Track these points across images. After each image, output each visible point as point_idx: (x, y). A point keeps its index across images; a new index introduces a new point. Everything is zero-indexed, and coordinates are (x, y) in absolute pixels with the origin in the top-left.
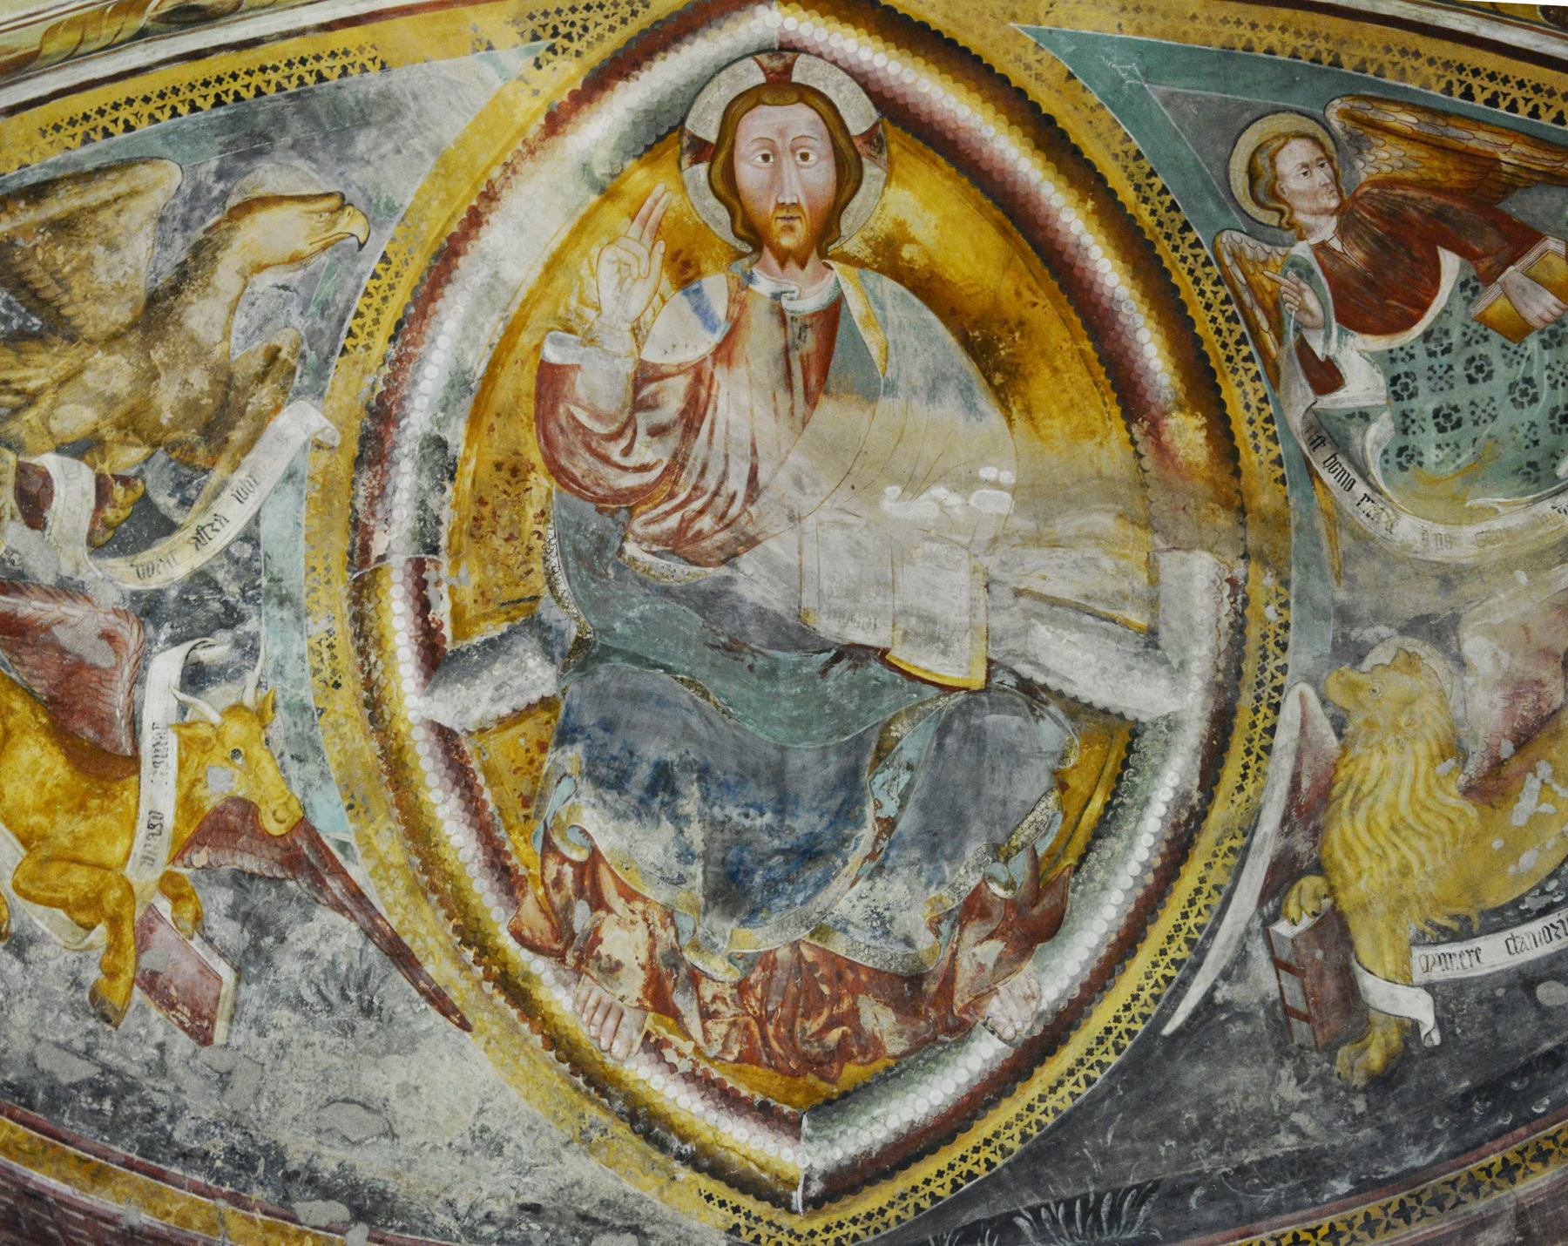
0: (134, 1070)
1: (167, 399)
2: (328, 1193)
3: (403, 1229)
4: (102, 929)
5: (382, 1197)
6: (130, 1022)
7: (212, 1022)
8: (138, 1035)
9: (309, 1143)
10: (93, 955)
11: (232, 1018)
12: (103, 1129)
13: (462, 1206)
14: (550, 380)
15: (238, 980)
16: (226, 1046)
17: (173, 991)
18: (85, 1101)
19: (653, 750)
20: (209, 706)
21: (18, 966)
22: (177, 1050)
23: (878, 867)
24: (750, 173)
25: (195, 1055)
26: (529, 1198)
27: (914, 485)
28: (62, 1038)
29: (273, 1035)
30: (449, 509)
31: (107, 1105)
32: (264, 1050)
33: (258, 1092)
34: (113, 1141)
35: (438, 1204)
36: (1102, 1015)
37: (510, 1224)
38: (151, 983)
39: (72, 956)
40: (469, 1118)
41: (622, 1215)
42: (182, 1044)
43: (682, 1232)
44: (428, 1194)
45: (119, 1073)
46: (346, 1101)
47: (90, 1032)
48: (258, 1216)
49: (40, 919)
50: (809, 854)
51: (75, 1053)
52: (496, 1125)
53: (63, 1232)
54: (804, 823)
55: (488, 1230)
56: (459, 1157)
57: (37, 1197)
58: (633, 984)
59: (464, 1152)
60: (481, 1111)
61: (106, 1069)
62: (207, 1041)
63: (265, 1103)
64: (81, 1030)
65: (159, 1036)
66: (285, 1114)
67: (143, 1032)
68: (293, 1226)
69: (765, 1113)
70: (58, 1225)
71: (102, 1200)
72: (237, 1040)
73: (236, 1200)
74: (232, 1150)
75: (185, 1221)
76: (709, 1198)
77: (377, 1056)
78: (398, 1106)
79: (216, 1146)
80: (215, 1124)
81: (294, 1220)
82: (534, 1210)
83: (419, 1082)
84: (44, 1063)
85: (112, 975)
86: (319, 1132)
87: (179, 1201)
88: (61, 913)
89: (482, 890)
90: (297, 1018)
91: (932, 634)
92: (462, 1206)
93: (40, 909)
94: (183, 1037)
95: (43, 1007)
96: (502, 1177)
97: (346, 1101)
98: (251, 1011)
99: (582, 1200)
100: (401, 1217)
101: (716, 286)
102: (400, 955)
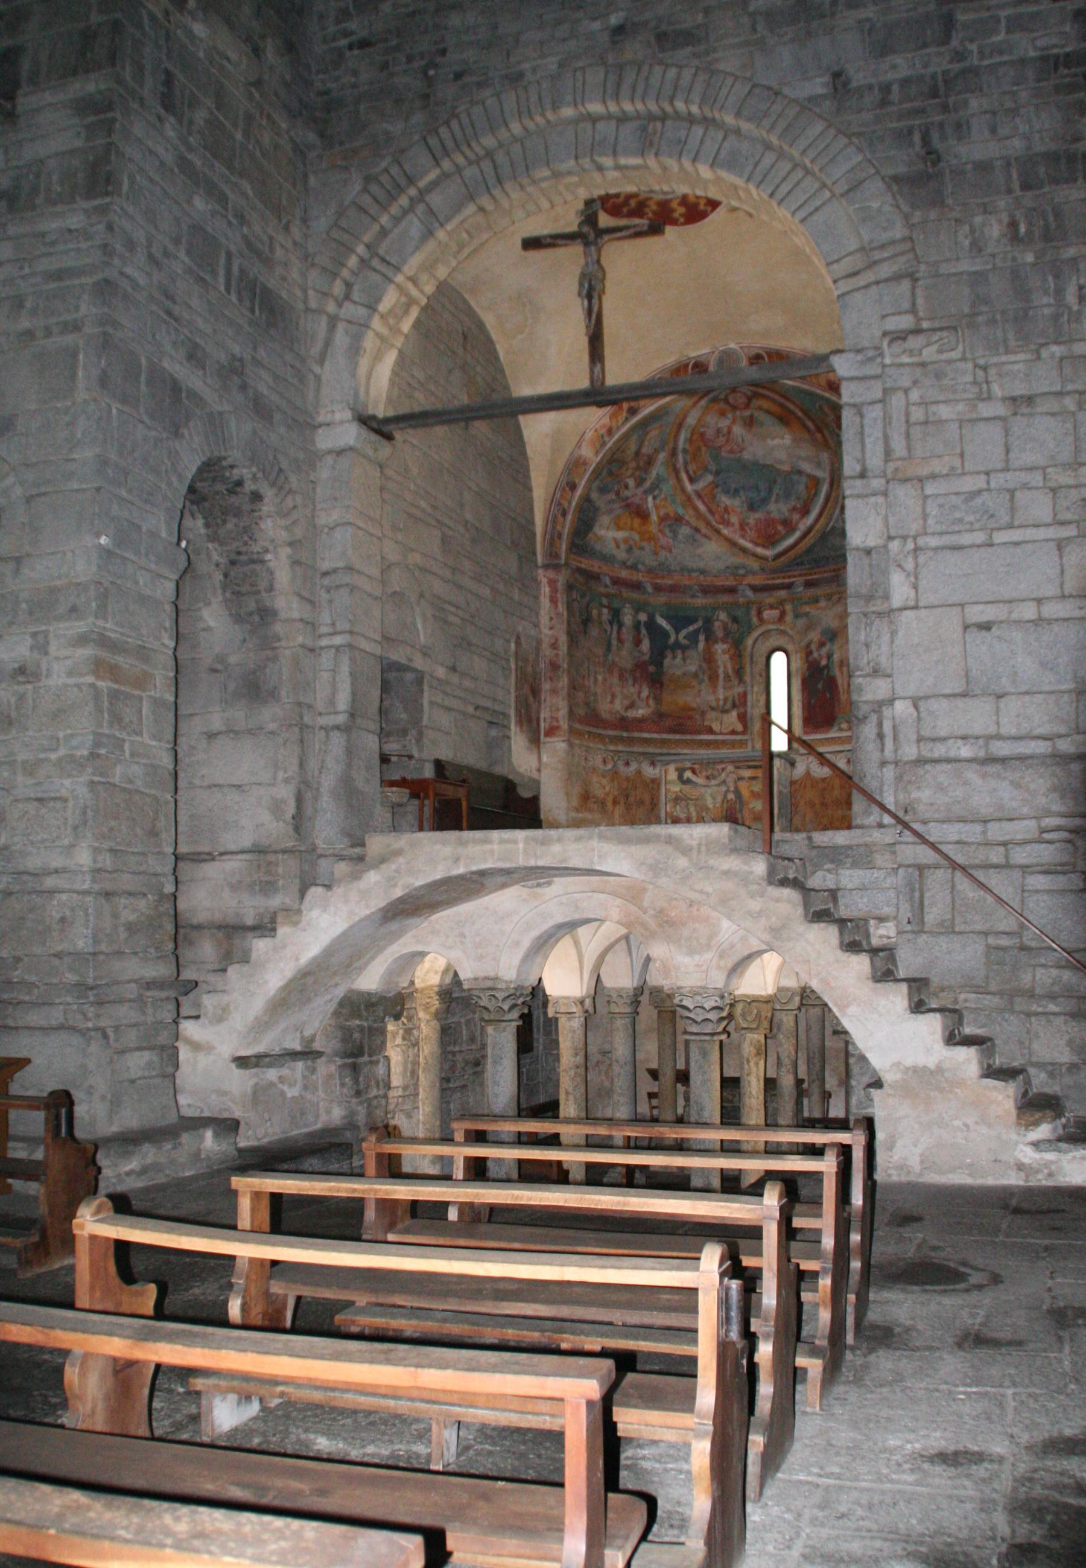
1: (641, 464)
14: (702, 435)
19: (733, 486)
20: (658, 501)
23: (777, 501)
24: (731, 400)
27: (773, 438)
30: (688, 457)
36: (818, 527)
38: (662, 547)
49: (644, 544)
50: (765, 501)
54: (763, 494)
58: (737, 526)
62: (670, 551)
69: (764, 546)
89: (708, 515)
91: (780, 462)
101: (730, 416)
102: (697, 530)
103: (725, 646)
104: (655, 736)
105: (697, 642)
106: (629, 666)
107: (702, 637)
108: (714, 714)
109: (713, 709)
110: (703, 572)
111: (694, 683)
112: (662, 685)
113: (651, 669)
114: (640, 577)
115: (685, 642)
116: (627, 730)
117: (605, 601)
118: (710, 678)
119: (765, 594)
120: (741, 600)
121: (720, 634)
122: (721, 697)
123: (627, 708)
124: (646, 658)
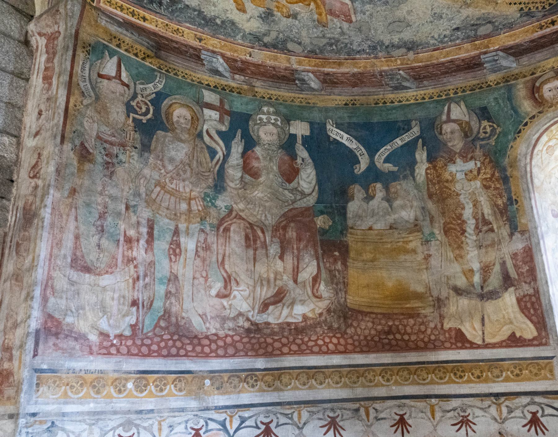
0: (337, 36)
2: (399, 47)
3: (422, 48)
4: (312, 4)
5: (413, 42)
6: (330, 25)
7: (350, 16)
8: (333, 27)
9: (389, 37)
10: (313, 11)
11: (355, 13)
12: (336, 53)
13: (436, 36)
15: (352, 3)
16: (356, 21)
17: (337, 12)
18: (329, 48)
21: (297, 22)
22: (345, 27)
25: (350, 26)
26: (455, 26)
28: (316, 35)
29: (368, 13)
31: (334, 47)
32: (367, 18)
33: (370, 29)
34: (339, 55)
35: (429, 38)
37: (452, 36)
38: (331, 12)
39: (309, 14)
40: (430, 12)
41: (484, 20)
42: (345, 25)
43: (505, 17)
44: (426, 37)
45: (334, 38)
46: (394, 22)
47: (322, 31)
48: (383, 59)
49: (297, 8)
51: (321, 38)
52: (438, 11)
53: (338, 79)
55: (446, 39)
56: (430, 24)
57: (328, 74)
59: (432, 22)
60: (432, 9)
61: (330, 39)
62: (351, 22)
63: (373, 32)
64: (319, 32)
65: (339, 25)
66: (379, 32)
67: (334, 26)
68: (393, 59)
70: (335, 79)
71: (344, 70)
72: (359, 18)
73: (376, 58)
74: (370, 46)
75: (365, 67)
76: (510, 4)
77: (398, 7)
78: (409, 18)
79: (365, 47)
80: (363, 41)
81: (392, 57)
82: (457, 29)
83: (412, 8)
84: (315, 42)
85: (320, 14)
86: (390, 33)
87: (362, 63)
88: (301, 4)
90: (372, 6)
92: (436, 36)
93: (295, 5)
94: (344, 23)
95: (308, 29)
96: (445, 24)
97: (394, 22)
98: (359, 9)
99: (470, 21)
100: (420, 45)
103: (471, 165)
104: (336, 360)
105: (413, 164)
106: (270, 220)
107: (421, 155)
108: (464, 302)
109: (458, 291)
110: (411, 46)
111: (415, 243)
112: (344, 250)
113: (321, 221)
114: (294, 63)
115: (389, 167)
116: (268, 355)
117: (209, 97)
118: (447, 231)
119: (538, 56)
120: (492, 78)
121: (457, 144)
122: (476, 266)
123: (265, 306)
124: (311, 201)
